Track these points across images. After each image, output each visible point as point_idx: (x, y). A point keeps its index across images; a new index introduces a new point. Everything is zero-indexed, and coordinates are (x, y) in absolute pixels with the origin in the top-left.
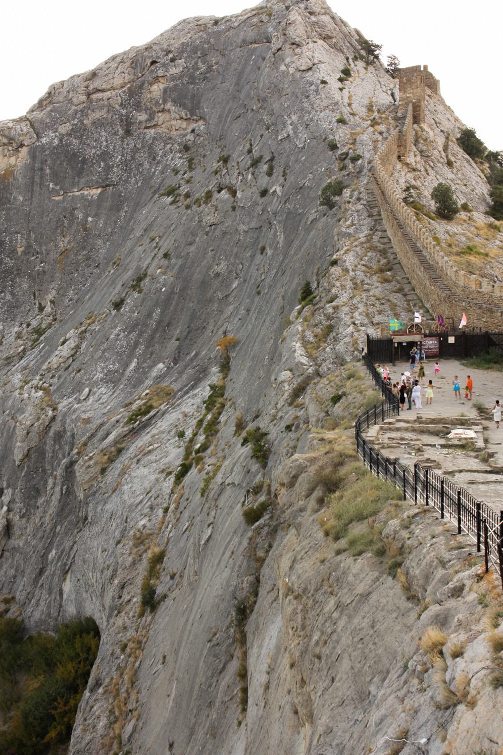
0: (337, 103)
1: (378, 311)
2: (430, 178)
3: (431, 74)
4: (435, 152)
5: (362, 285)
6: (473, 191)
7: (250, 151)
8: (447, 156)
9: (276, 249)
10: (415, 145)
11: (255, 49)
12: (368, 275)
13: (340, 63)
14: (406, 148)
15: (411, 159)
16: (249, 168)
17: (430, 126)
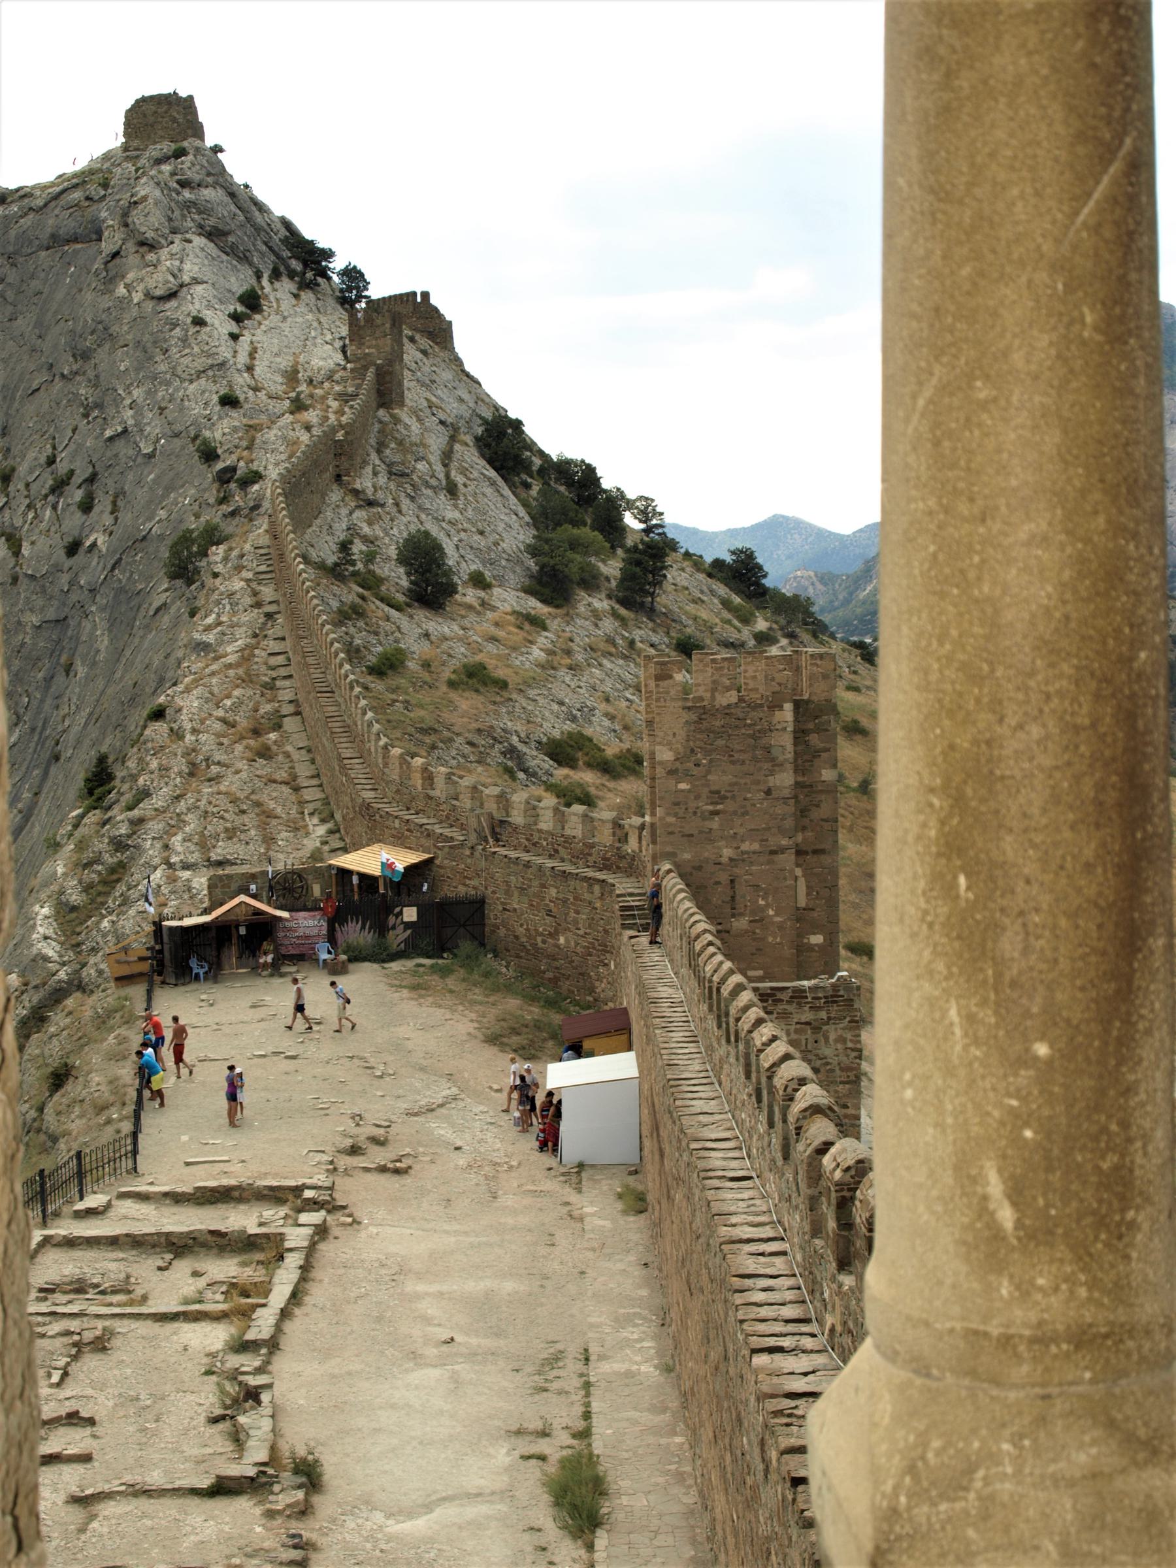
0: (222, 364)
1: (227, 830)
2: (405, 520)
3: (436, 310)
4: (421, 466)
5: (208, 767)
6: (496, 544)
7: (51, 461)
8: (448, 476)
9: (94, 664)
10: (379, 452)
11: (76, 252)
12: (225, 741)
13: (240, 281)
14: (351, 458)
15: (365, 482)
16: (46, 496)
17: (416, 413)
